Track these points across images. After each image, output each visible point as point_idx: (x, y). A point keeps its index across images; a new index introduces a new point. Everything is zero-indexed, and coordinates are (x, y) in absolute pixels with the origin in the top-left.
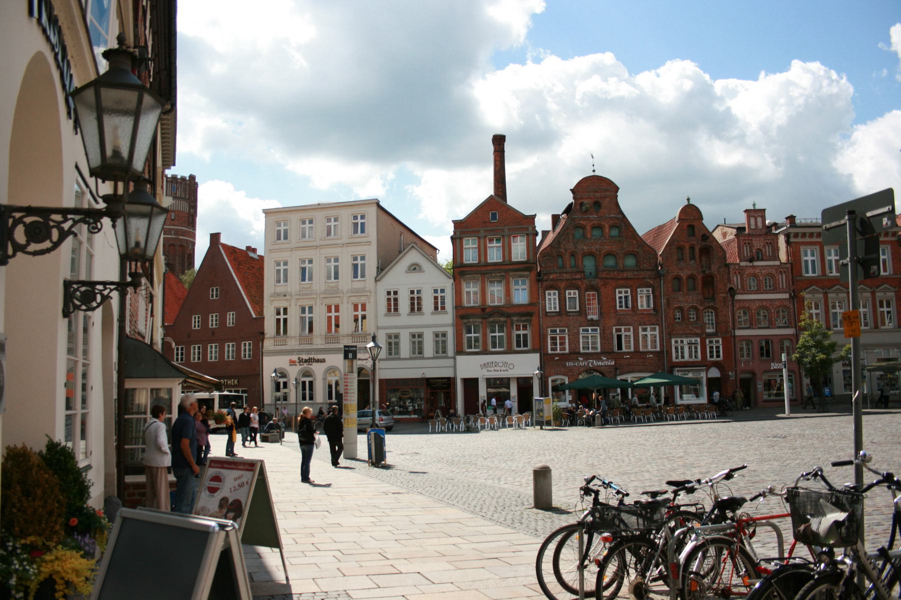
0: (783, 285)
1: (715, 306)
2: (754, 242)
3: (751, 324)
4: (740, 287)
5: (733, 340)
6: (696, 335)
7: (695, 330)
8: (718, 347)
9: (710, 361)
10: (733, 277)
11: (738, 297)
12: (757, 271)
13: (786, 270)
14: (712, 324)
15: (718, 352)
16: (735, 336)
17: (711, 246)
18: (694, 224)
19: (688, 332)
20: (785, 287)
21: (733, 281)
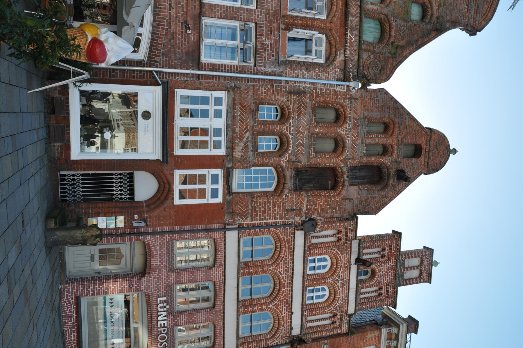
0: (313, 321)
1: (286, 191)
2: (385, 266)
3: (246, 265)
4: (314, 241)
5: (216, 226)
6: (230, 148)
7: (242, 144)
8: (202, 194)
9: (173, 175)
10: (333, 228)
11: (300, 236)
12: (340, 272)
13: (338, 324)
14: (249, 186)
15: (192, 194)
16: (225, 230)
17: (386, 186)
18: (422, 158)
19: (237, 130)
20: (309, 325)
21: (326, 229)
